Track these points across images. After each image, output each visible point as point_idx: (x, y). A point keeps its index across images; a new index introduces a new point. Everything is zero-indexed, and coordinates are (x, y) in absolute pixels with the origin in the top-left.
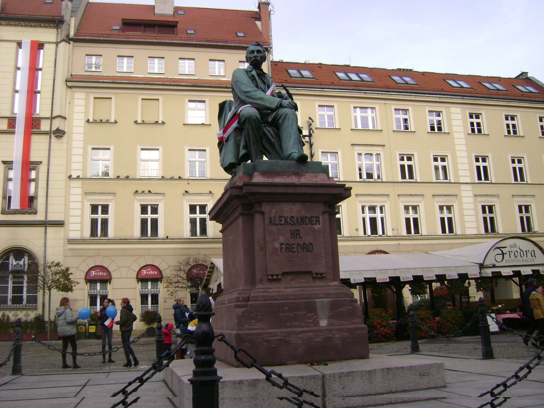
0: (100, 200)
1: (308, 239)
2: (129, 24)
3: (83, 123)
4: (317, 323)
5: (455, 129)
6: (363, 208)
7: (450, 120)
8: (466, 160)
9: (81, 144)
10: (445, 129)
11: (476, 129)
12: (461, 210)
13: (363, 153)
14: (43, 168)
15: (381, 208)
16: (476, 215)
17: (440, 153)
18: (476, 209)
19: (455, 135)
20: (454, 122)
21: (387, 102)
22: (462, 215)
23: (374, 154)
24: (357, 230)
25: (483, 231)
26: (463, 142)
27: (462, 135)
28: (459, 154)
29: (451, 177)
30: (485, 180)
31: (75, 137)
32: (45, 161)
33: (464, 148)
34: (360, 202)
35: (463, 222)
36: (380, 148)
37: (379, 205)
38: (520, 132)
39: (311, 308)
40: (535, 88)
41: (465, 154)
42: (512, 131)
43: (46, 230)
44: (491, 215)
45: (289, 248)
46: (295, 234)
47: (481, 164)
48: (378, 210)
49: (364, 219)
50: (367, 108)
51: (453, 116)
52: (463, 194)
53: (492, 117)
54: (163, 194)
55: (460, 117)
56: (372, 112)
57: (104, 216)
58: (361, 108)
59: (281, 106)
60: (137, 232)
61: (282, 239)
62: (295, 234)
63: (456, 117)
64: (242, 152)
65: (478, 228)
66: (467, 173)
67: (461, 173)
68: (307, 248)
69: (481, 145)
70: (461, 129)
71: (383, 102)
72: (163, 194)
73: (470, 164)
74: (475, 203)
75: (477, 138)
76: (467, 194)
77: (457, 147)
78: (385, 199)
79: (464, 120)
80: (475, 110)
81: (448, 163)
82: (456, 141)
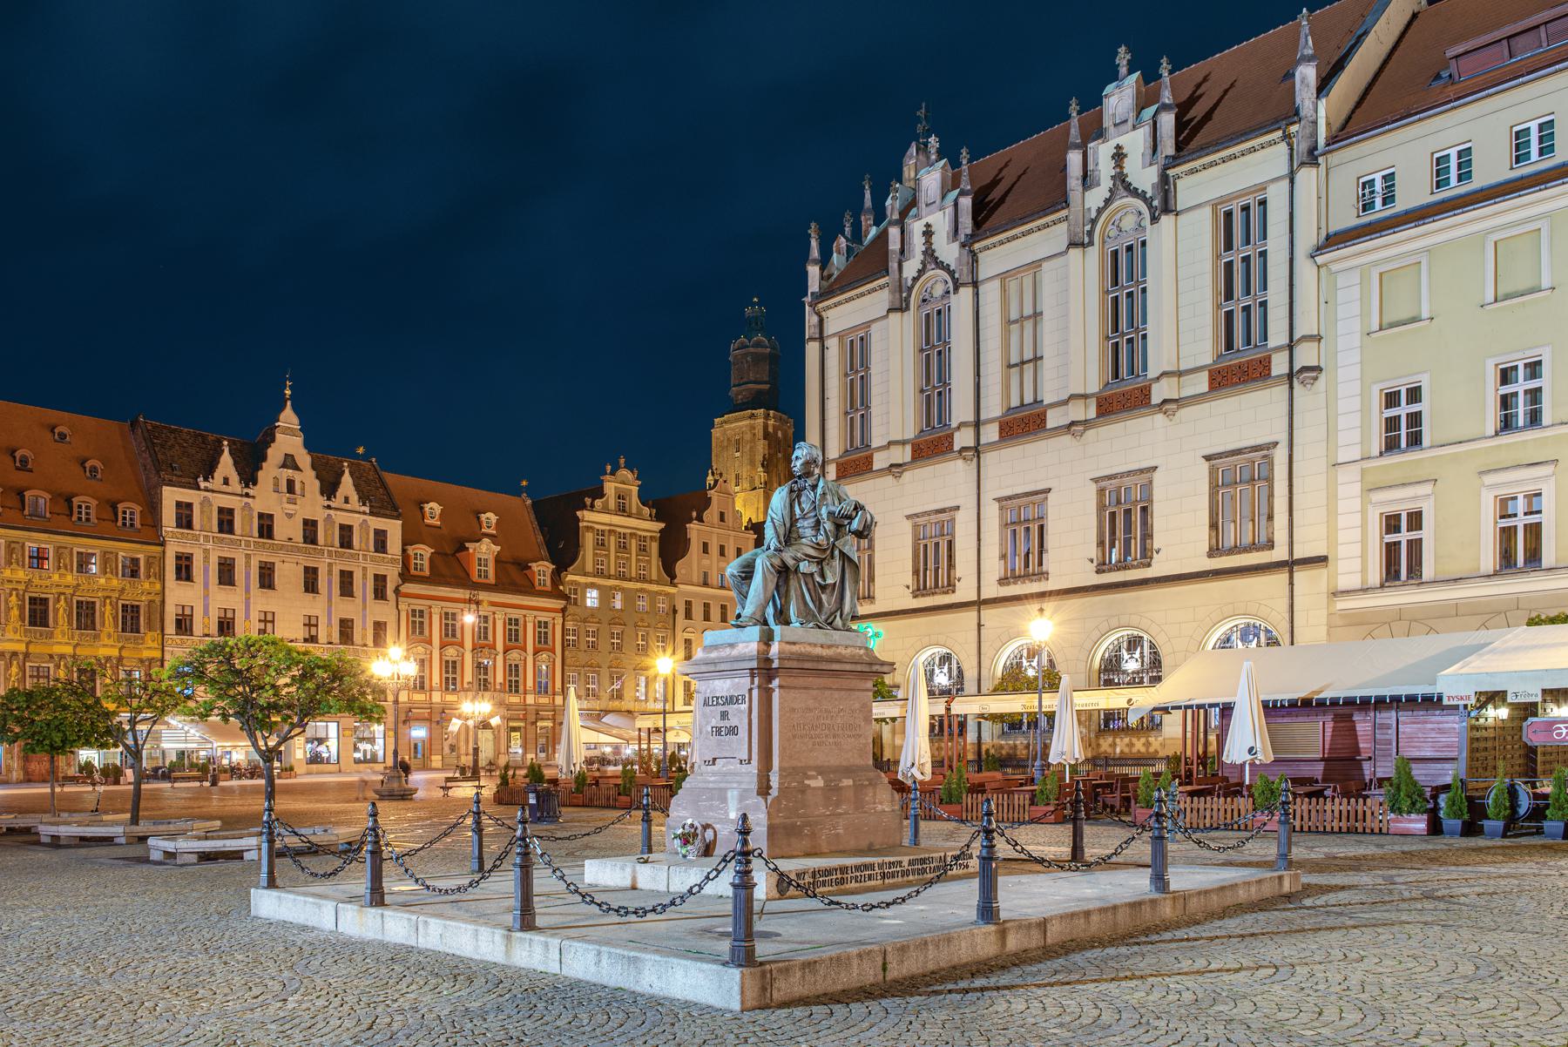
0: (1399, 501)
1: (733, 722)
3: (1356, 340)
4: (727, 813)
9: (1356, 387)
14: (1280, 456)
31: (1342, 374)
32: (1283, 438)
39: (724, 800)
43: (1291, 577)
45: (718, 731)
46: (724, 715)
57: (1414, 535)
60: (1488, 558)
61: (714, 722)
62: (724, 715)
68: (733, 731)
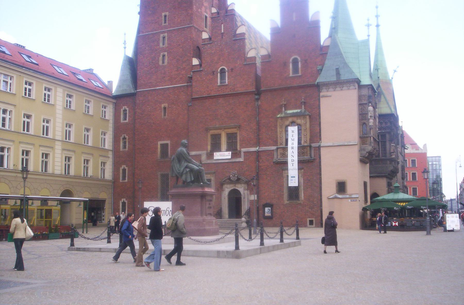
10: (52, 102)
12: (54, 157)
15: (8, 149)
16: (62, 162)
18: (62, 158)
20: (58, 98)
21: (22, 75)
22: (54, 162)
23: (9, 110)
25: (64, 173)
29: (50, 136)
30: (69, 140)
35: (54, 165)
37: (7, 147)
48: (6, 151)
50: (8, 75)
52: (57, 147)
58: (5, 75)
65: (61, 170)
71: (20, 74)
73: (63, 128)
74: (62, 154)
76: (58, 147)
78: (11, 143)
79: (63, 98)
81: (51, 125)
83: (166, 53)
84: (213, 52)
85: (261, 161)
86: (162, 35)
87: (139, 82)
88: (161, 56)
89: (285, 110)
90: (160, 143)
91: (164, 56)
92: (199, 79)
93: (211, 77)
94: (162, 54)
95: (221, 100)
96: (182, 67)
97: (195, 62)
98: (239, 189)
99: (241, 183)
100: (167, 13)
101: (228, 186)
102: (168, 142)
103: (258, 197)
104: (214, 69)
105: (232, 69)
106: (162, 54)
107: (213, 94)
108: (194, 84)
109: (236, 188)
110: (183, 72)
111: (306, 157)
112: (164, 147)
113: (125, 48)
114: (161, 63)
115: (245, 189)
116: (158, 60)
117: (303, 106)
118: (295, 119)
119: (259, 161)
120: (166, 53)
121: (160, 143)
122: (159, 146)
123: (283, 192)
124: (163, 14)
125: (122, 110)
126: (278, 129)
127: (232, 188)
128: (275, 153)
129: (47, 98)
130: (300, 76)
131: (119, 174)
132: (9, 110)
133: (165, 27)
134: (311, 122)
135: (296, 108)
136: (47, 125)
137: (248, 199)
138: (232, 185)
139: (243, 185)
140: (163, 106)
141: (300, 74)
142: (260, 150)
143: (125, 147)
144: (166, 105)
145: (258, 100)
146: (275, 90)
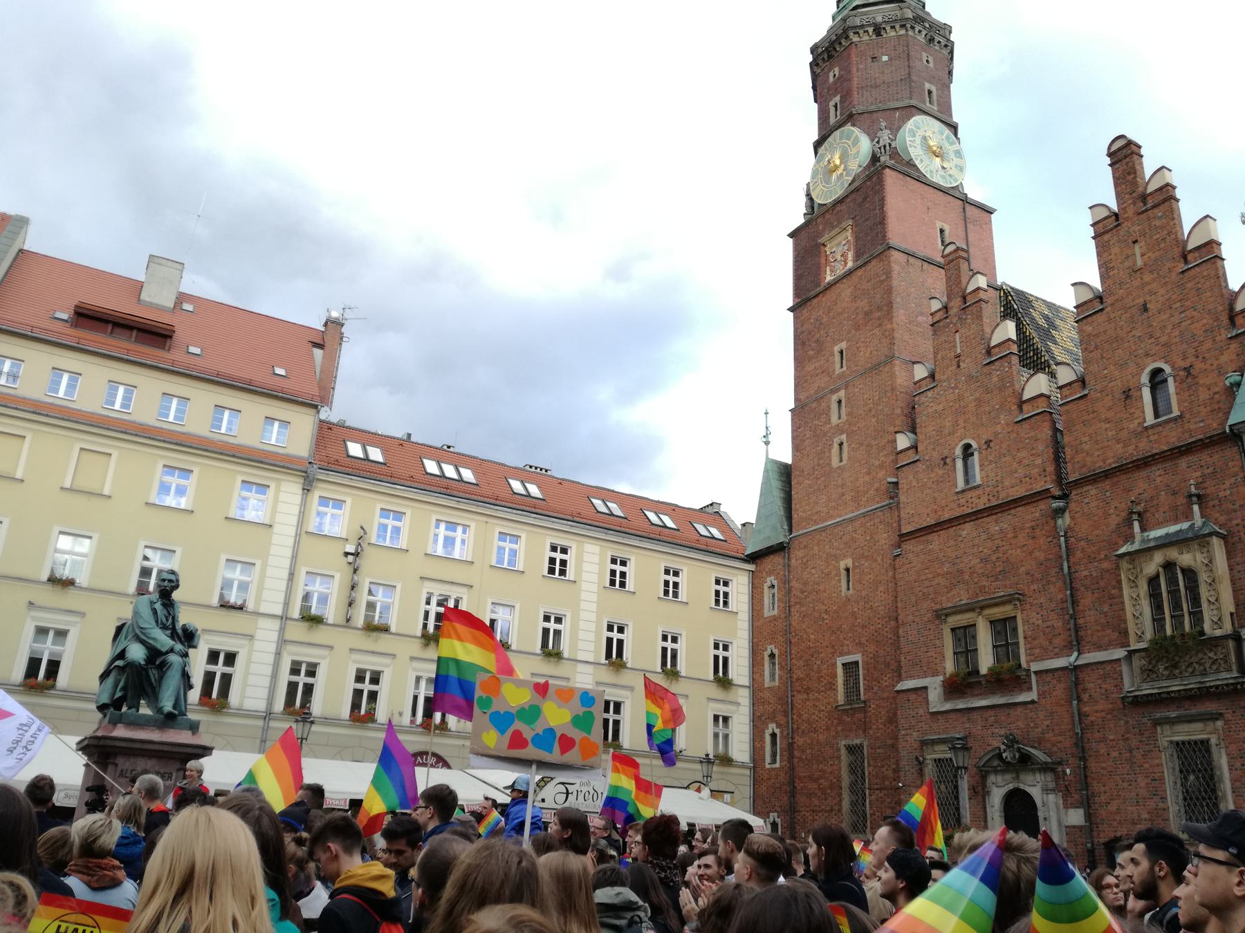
2: (86, 317)
5: (585, 576)
6: (418, 679)
7: (580, 560)
8: (593, 627)
11: (617, 580)
13: (437, 593)
17: (555, 610)
19: (584, 586)
20: (586, 567)
21: (490, 520)
24: (401, 714)
26: (594, 598)
27: (595, 588)
28: (583, 615)
33: (594, 607)
34: (415, 669)
36: (465, 590)
38: (683, 595)
40: (722, 532)
41: (593, 617)
42: (672, 590)
44: (617, 717)
47: (615, 635)
49: (416, 698)
51: (586, 557)
53: (646, 568)
54: (82, 615)
55: (596, 559)
56: (464, 532)
59: (172, 650)
63: (590, 558)
64: (118, 694)
66: (591, 647)
67: (581, 645)
69: (619, 606)
70: (595, 578)
72: (82, 615)
73: (598, 633)
75: (616, 595)
77: (583, 605)
80: (621, 553)
82: (583, 596)
83: (844, 437)
84: (941, 407)
85: (1085, 697)
86: (835, 397)
87: (795, 516)
88: (836, 446)
89: (1143, 529)
90: (840, 661)
91: (841, 444)
92: (914, 483)
93: (941, 472)
94: (836, 441)
95: (967, 530)
96: (877, 463)
97: (903, 442)
98: (1028, 789)
99: (1033, 771)
100: (843, 345)
101: (999, 778)
102: (858, 657)
103: (1088, 816)
104: (946, 452)
105: (988, 442)
106: (836, 441)
107: (947, 516)
108: (903, 498)
109: (1022, 787)
110: (881, 474)
111: (1224, 675)
112: (851, 668)
113: (767, 443)
114: (835, 462)
115: (1046, 790)
116: (830, 458)
117: (1196, 508)
118: (1173, 554)
119: (1079, 699)
120: (844, 437)
121: (840, 661)
122: (840, 671)
123: (1164, 799)
124: (837, 349)
125: (766, 586)
126: (1126, 592)
127: (1011, 786)
128: (1125, 669)
129: (557, 568)
130: (1175, 419)
131: (763, 748)
132: (454, 596)
133: (841, 376)
134: (1230, 554)
135: (1176, 520)
136: (621, 636)
137: (1060, 824)
138: (1008, 777)
139: (1039, 777)
140: (842, 565)
141: (1176, 413)
142: (1080, 662)
143: (772, 675)
144: (848, 562)
145: (1060, 512)
146: (1107, 474)
